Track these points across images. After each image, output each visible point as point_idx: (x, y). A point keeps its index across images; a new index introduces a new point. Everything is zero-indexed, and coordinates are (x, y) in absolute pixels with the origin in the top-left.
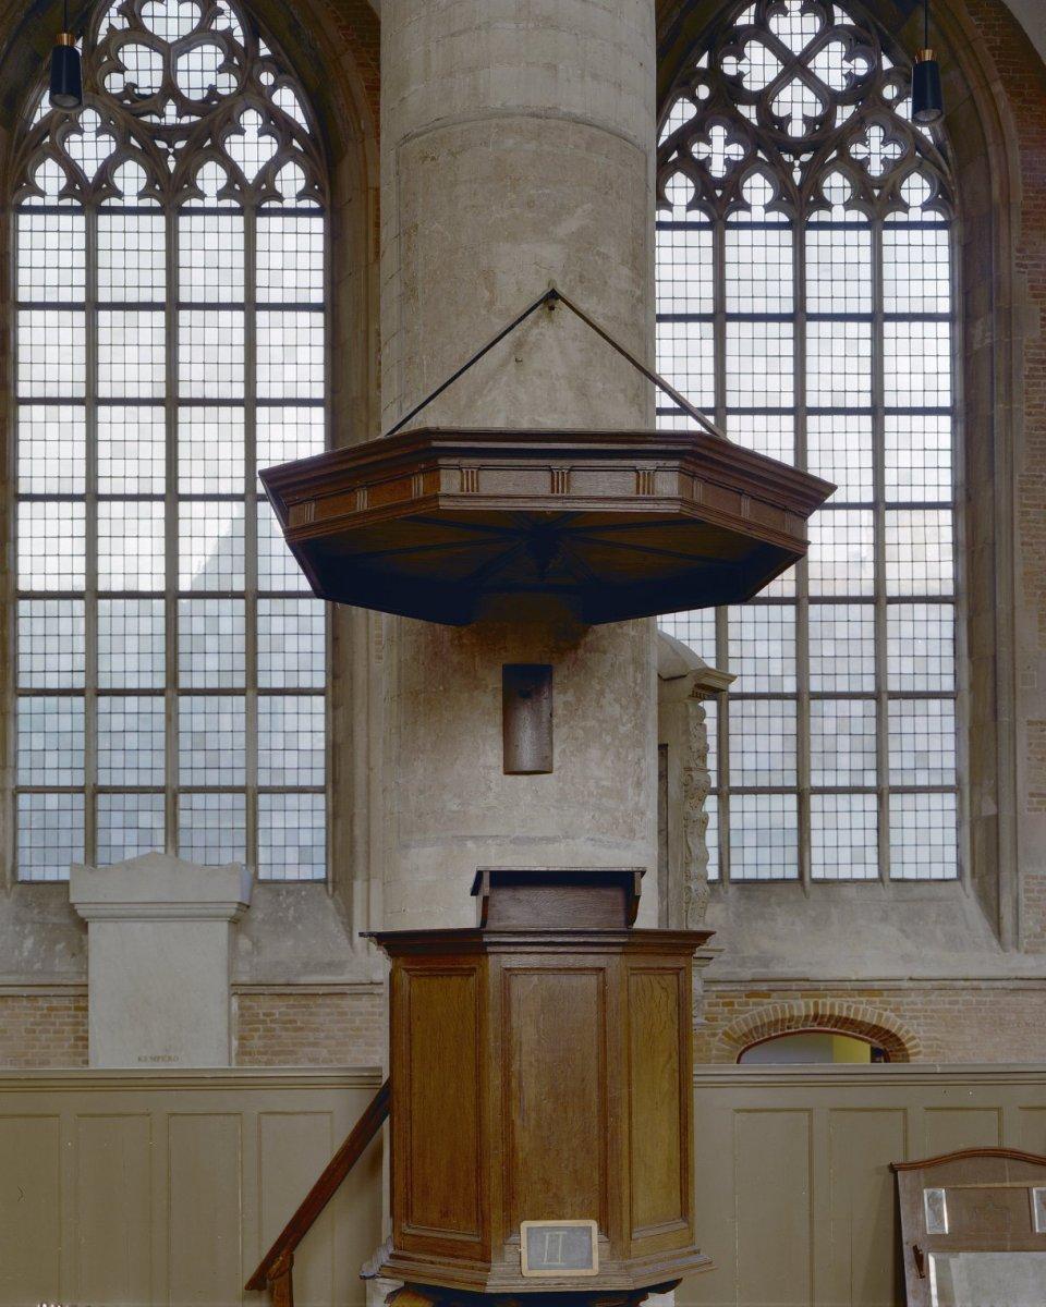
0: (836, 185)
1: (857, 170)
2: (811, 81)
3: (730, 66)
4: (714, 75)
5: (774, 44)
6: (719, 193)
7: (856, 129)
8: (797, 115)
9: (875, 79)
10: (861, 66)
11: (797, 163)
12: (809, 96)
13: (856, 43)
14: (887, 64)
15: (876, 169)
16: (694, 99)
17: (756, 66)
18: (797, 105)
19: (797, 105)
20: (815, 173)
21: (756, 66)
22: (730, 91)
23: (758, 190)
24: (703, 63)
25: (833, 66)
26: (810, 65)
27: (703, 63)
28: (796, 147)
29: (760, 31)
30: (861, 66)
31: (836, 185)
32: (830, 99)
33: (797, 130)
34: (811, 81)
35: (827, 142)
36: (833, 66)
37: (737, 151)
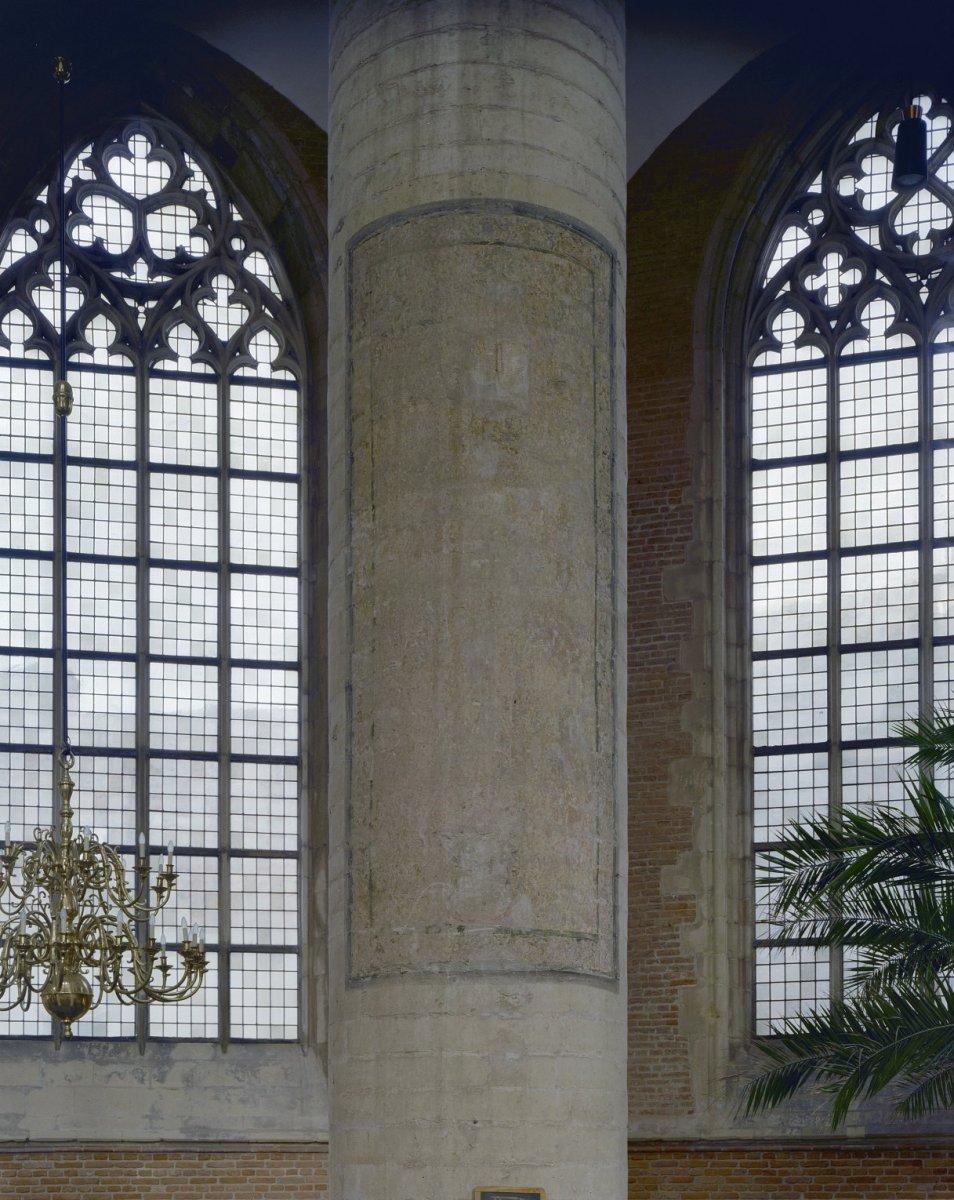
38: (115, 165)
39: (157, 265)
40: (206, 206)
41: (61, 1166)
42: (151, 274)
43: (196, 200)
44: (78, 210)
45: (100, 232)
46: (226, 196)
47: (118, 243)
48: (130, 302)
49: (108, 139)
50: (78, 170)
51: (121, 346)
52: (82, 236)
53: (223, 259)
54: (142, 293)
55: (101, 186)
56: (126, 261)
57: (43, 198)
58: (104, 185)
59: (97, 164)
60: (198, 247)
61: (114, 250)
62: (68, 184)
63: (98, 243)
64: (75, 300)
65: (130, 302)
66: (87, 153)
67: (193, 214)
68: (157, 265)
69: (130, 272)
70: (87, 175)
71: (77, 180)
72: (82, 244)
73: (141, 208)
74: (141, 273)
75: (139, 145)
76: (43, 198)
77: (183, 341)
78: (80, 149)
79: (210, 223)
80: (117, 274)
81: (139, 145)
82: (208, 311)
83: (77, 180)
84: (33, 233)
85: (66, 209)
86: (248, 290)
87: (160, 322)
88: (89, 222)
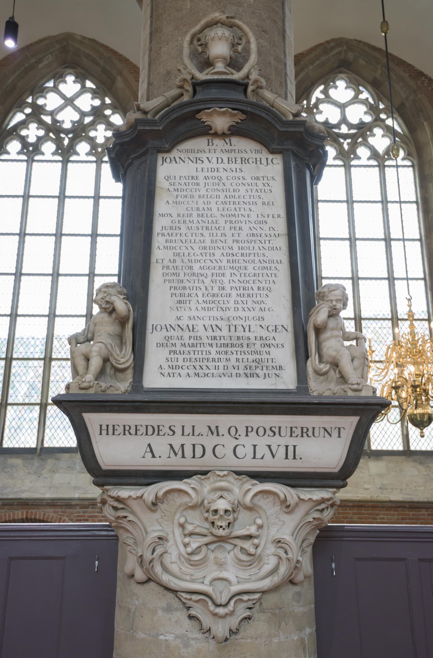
3: (40, 102)
4: (34, 105)
6: (31, 149)
7: (93, 125)
9: (103, 106)
10: (97, 103)
13: (95, 93)
16: (24, 113)
24: (30, 100)
28: (67, 132)
29: (55, 89)
30: (97, 103)
32: (83, 114)
33: (67, 125)
34: (77, 109)
37: (41, 133)
38: (332, 92)
39: (350, 126)
40: (370, 103)
41: (341, 513)
43: (365, 102)
44: (317, 108)
47: (334, 119)
50: (318, 94)
51: (338, 157)
54: (345, 136)
56: (338, 126)
58: (328, 99)
59: (325, 92)
60: (368, 119)
62: (313, 101)
68: (350, 126)
70: (322, 96)
71: (318, 99)
73: (343, 107)
74: (344, 129)
83: (318, 99)
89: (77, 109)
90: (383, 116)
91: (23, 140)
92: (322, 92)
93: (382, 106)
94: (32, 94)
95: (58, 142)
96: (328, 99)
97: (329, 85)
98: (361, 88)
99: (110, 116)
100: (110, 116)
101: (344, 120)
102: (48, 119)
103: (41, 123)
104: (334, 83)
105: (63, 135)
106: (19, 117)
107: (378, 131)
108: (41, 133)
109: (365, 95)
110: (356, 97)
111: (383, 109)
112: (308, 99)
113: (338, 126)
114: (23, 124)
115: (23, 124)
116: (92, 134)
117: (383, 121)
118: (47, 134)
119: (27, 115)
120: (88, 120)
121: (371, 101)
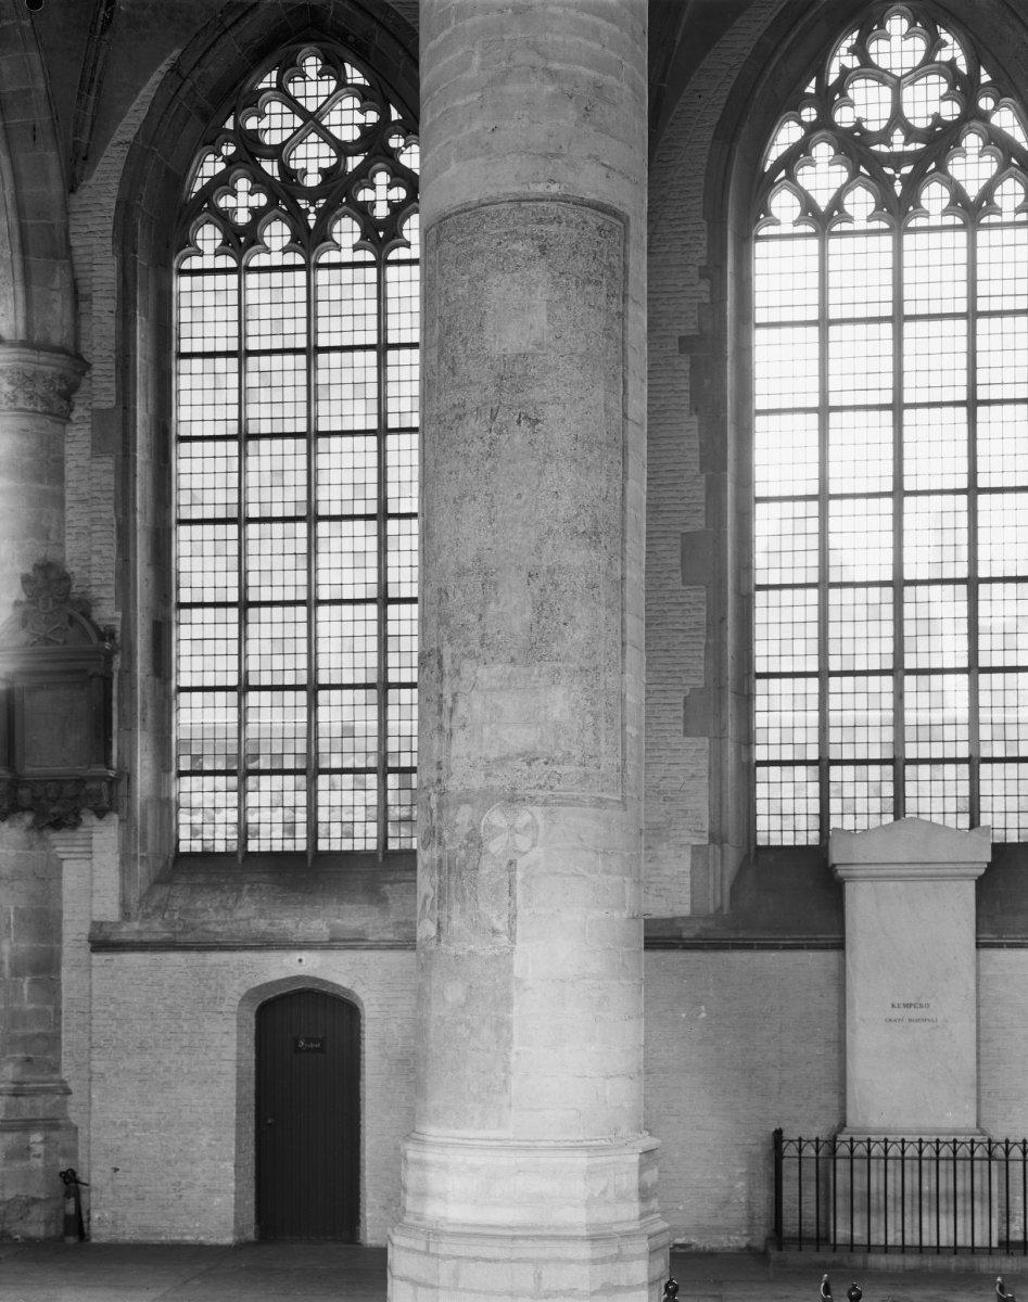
0: (347, 231)
1: (363, 212)
2: (298, 137)
5: (292, 103)
7: (364, 176)
8: (312, 167)
11: (312, 209)
12: (325, 149)
14: (395, 115)
15: (381, 211)
17: (274, 124)
18: (312, 159)
19: (312, 159)
20: (325, 217)
21: (274, 124)
22: (250, 148)
23: (277, 234)
24: (229, 125)
25: (348, 120)
26: (325, 122)
27: (229, 125)
28: (314, 196)
31: (347, 231)
32: (343, 149)
33: (312, 180)
34: (327, 137)
35: (339, 189)
36: (348, 120)
39: (911, 134)
42: (906, 143)
45: (860, 112)
46: (975, 61)
48: (889, 171)
49: (869, 23)
50: (843, 58)
52: (844, 117)
53: (971, 115)
54: (898, 160)
55: (865, 70)
56: (884, 136)
57: (811, 89)
58: (868, 68)
59: (860, 50)
60: (950, 110)
61: (873, 127)
62: (833, 76)
63: (859, 123)
64: (840, 175)
65: (889, 171)
66: (848, 43)
67: (943, 80)
68: (911, 134)
69: (889, 144)
70: (853, 62)
72: (844, 125)
75: (897, 25)
76: (811, 89)
77: (934, 196)
78: (845, 37)
79: (964, 88)
80: (876, 148)
81: (897, 25)
82: (958, 168)
84: (801, 123)
85: (828, 100)
86: (997, 141)
87: (914, 184)
88: (852, 104)
89: (327, 137)
90: (986, 103)
91: (223, 219)
92: (853, 51)
93: (985, 78)
94: (234, 111)
95: (295, 218)
96: (868, 68)
97: (871, 31)
98: (946, 36)
99: (399, 151)
100: (399, 151)
101: (897, 118)
102: (270, 167)
103: (260, 182)
104: (882, 26)
105: (303, 204)
106: (212, 167)
107: (972, 141)
108: (261, 200)
109: (953, 51)
110: (928, 59)
111: (988, 84)
112: (821, 73)
113: (884, 136)
114: (223, 183)
115: (223, 183)
116: (364, 195)
117: (984, 117)
118: (272, 204)
119: (229, 160)
120: (354, 162)
121: (962, 65)
